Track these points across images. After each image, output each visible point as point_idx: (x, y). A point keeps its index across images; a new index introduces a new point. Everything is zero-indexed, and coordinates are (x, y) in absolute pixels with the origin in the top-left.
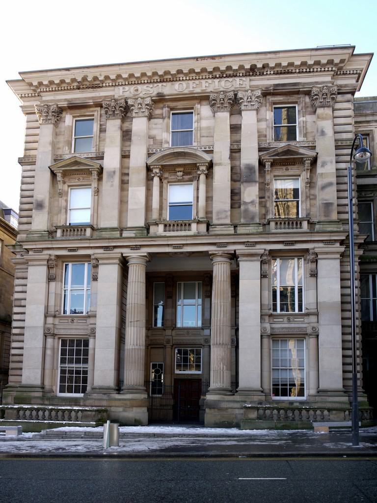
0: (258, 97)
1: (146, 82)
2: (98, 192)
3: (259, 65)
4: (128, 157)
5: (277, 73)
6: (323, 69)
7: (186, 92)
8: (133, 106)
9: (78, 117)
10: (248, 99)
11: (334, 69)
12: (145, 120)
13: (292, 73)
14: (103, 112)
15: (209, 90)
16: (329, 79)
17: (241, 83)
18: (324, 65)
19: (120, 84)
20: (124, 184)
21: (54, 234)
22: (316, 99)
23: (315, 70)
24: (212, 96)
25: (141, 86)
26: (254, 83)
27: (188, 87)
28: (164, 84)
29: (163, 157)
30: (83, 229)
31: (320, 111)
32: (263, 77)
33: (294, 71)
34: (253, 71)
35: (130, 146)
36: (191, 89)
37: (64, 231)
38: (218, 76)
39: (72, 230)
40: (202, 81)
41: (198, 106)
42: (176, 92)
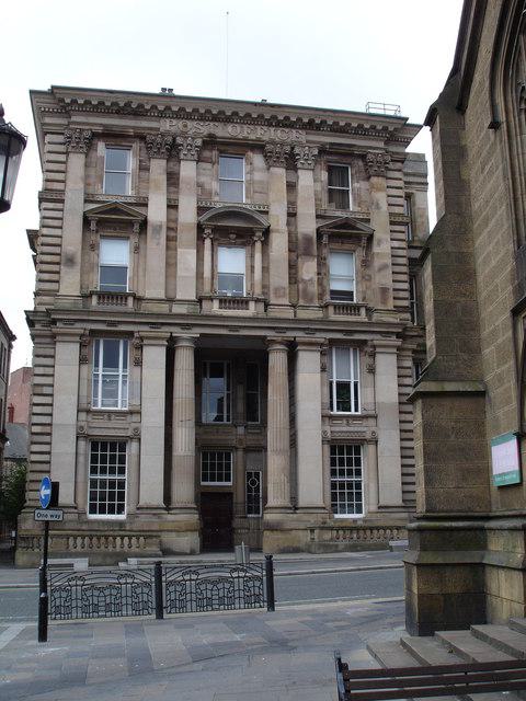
3: (318, 121)
13: (347, 132)
16: (382, 145)
18: (379, 131)
20: (171, 240)
24: (269, 147)
26: (311, 138)
31: (374, 180)
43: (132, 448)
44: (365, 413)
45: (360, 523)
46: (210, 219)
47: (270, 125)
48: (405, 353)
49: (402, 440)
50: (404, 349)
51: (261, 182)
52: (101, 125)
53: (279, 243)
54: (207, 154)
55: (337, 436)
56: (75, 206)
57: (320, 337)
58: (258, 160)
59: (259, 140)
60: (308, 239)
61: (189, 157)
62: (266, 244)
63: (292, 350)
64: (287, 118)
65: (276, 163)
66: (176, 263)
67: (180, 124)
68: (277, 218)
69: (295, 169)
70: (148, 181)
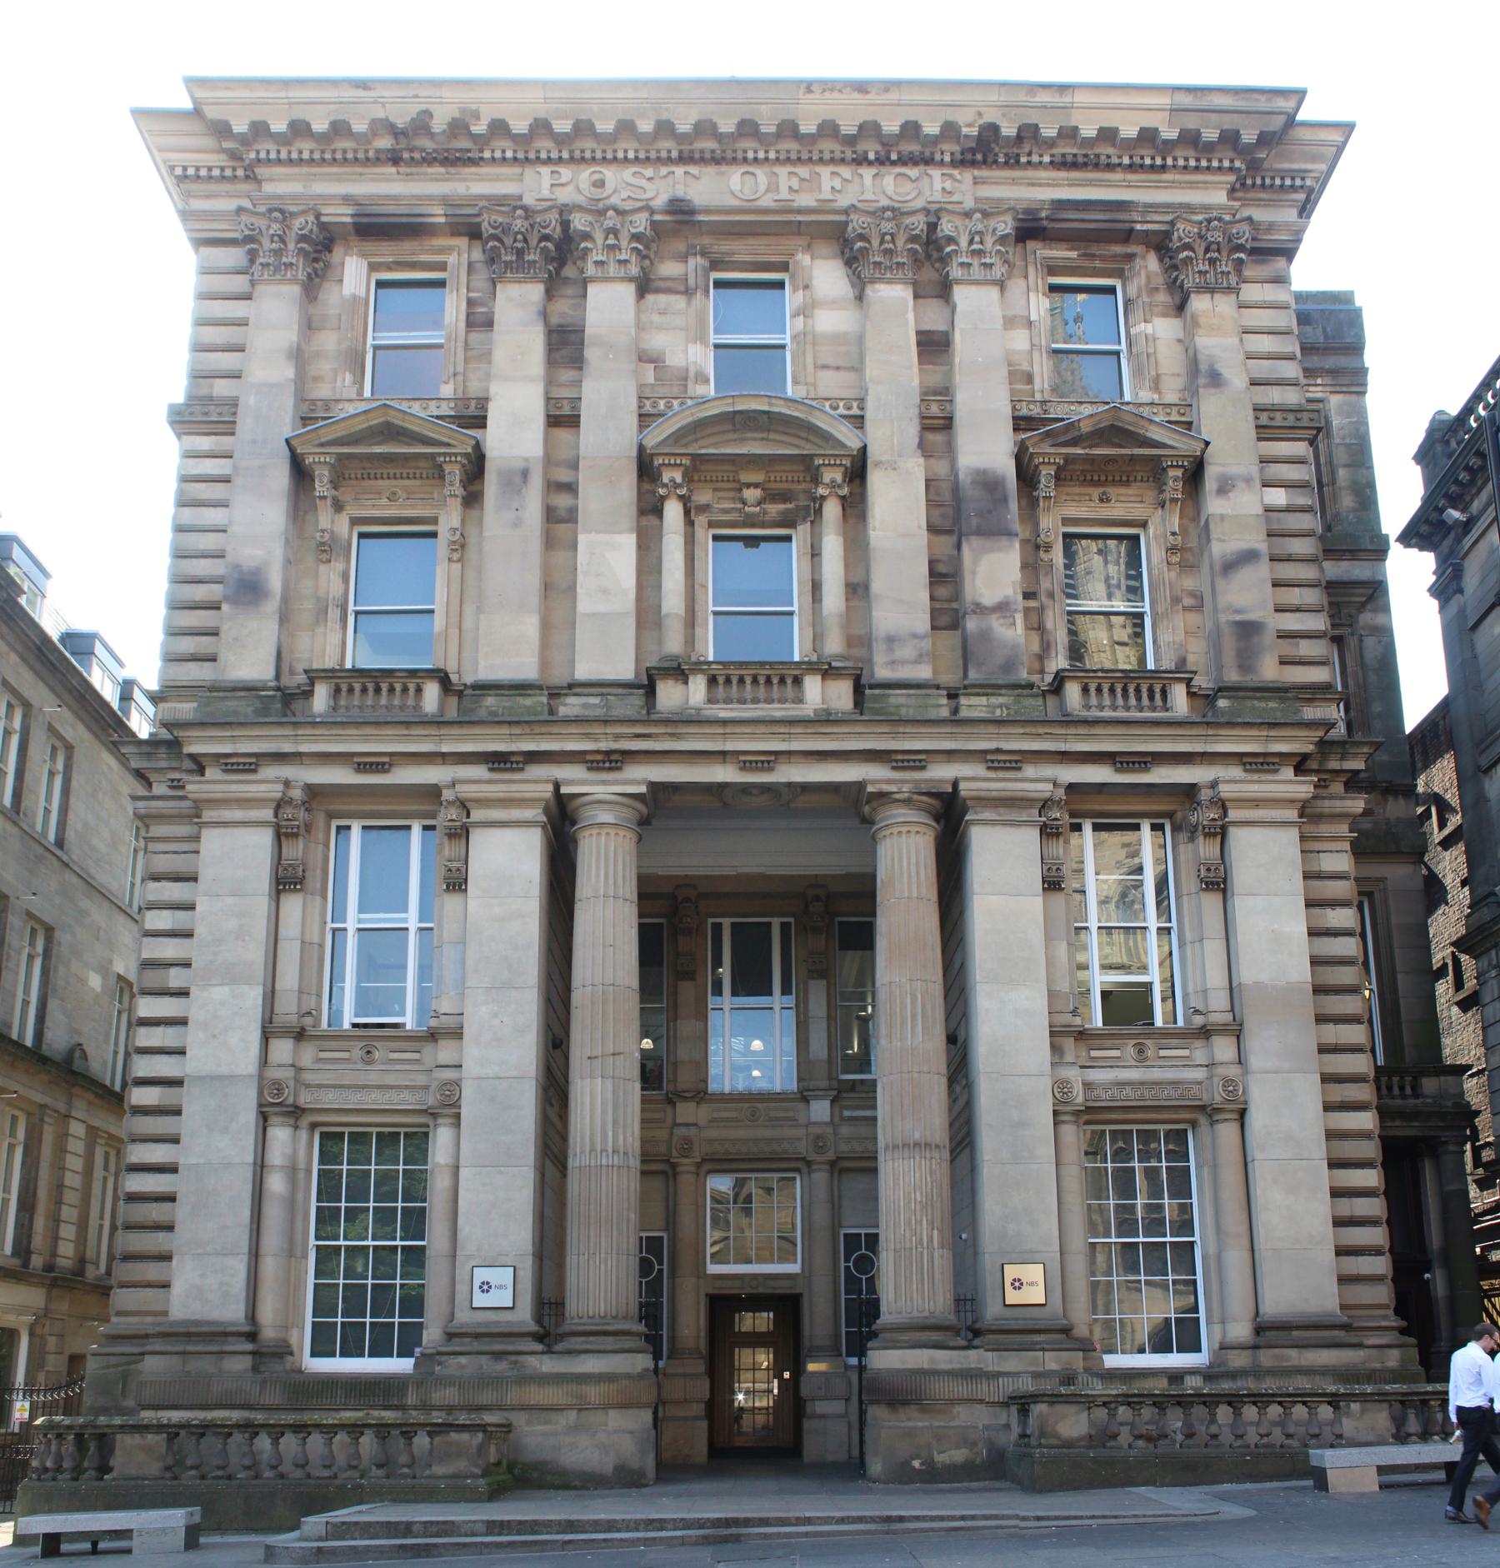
0: (1002, 240)
1: (631, 155)
2: (463, 546)
6: (1204, 163)
7: (767, 202)
8: (587, 236)
9: (389, 267)
10: (971, 242)
11: (1237, 164)
12: (628, 291)
13: (1110, 167)
14: (477, 255)
15: (843, 202)
16: (1220, 197)
17: (948, 185)
18: (1209, 148)
19: (543, 155)
21: (297, 705)
23: (1181, 162)
25: (613, 168)
27: (773, 187)
29: (698, 428)
30: (412, 688)
32: (1017, 174)
33: (1115, 160)
34: (984, 150)
35: (578, 383)
36: (784, 194)
37: (338, 690)
38: (871, 156)
39: (371, 687)
40: (818, 169)
41: (804, 259)
42: (735, 203)
43: (442, 1140)
44: (1198, 1020)
45: (1193, 1383)
46: (678, 436)
47: (861, 161)
48: (1325, 829)
49: (1328, 1107)
50: (1317, 818)
52: (347, 199)
53: (898, 503)
54: (669, 269)
55: (1104, 1098)
56: (269, 421)
57: (1039, 780)
58: (826, 275)
59: (823, 207)
60: (989, 484)
61: (612, 269)
62: (855, 505)
65: (886, 271)
66: (572, 588)
67: (586, 175)
68: (891, 435)
69: (943, 290)
70: (486, 357)
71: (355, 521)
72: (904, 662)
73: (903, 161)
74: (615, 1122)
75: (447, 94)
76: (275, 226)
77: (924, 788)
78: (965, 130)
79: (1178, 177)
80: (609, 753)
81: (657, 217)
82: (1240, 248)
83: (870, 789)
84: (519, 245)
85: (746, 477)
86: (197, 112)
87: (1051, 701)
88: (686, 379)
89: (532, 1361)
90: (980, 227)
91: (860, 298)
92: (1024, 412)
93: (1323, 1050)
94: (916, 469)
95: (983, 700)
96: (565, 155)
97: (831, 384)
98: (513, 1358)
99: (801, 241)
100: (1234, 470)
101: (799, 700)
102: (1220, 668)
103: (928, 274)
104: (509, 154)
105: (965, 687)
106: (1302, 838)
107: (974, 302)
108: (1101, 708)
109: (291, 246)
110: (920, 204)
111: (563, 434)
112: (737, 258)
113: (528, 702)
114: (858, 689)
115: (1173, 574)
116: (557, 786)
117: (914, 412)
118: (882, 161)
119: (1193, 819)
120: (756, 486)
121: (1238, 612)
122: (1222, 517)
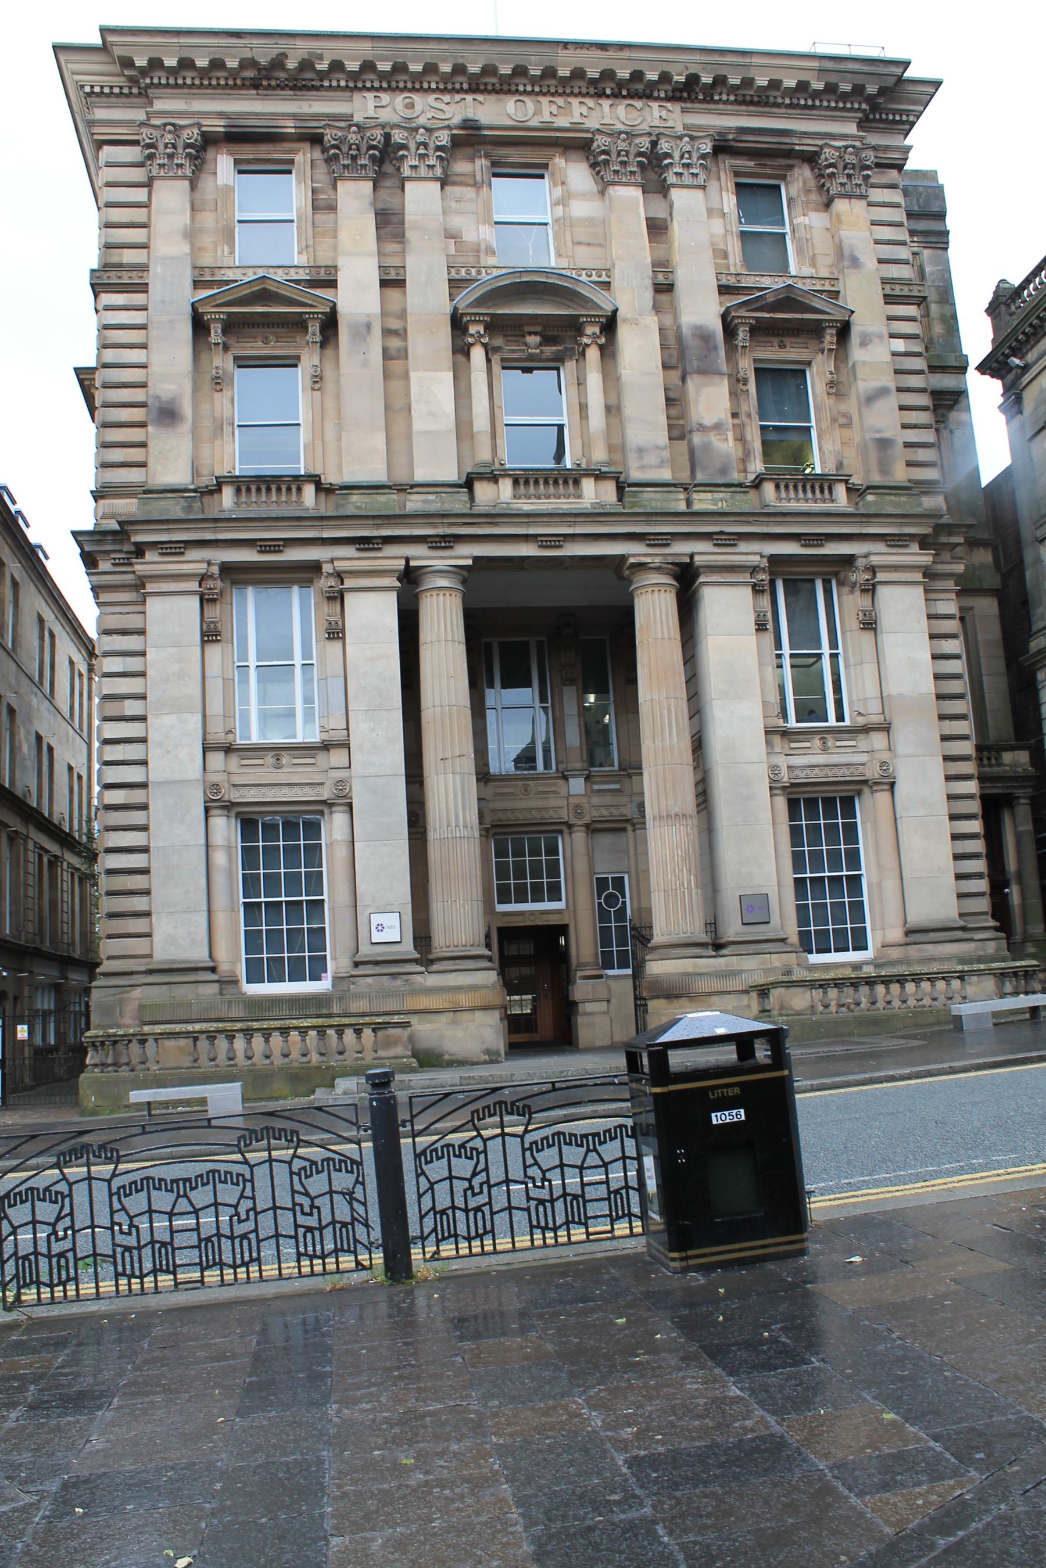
0: (703, 157)
3: (707, 79)
4: (400, 283)
5: (743, 103)
7: (534, 123)
8: (404, 147)
10: (682, 157)
13: (776, 105)
16: (852, 129)
17: (664, 114)
22: (832, 175)
24: (601, 142)
25: (420, 94)
28: (480, 97)
32: (712, 106)
33: (780, 100)
34: (688, 91)
36: (547, 118)
40: (570, 99)
42: (512, 123)
43: (334, 828)
44: (861, 721)
45: (869, 970)
46: (480, 301)
47: (600, 95)
48: (940, 585)
49: (948, 778)
51: (590, 221)
52: (221, 115)
53: (639, 347)
54: (461, 167)
55: (802, 777)
58: (577, 173)
59: (575, 127)
60: (704, 336)
61: (423, 172)
62: (608, 351)
63: (686, 581)
64: (637, 76)
67: (400, 99)
68: (630, 297)
69: (664, 189)
71: (236, 358)
72: (650, 467)
73: (631, 96)
74: (464, 806)
75: (300, 43)
76: (170, 136)
77: (670, 559)
78: (676, 78)
79: (823, 113)
80: (443, 537)
81: (455, 132)
82: (868, 168)
83: (632, 560)
84: (354, 153)
85: (527, 329)
86: (104, 48)
87: (753, 494)
88: (478, 251)
89: (419, 979)
90: (688, 148)
91: (602, 193)
92: (724, 282)
93: (944, 738)
94: (652, 322)
95: (709, 496)
96: (385, 85)
97: (585, 257)
98: (405, 977)
99: (561, 150)
100: (871, 329)
101: (580, 497)
102: (867, 471)
103: (652, 176)
104: (343, 83)
105: (696, 486)
106: (926, 591)
107: (685, 201)
108: (789, 500)
109: (180, 150)
110: (645, 127)
111: (393, 293)
112: (510, 160)
113: (383, 499)
114: (620, 489)
115: (831, 401)
116: (407, 560)
117: (649, 283)
118: (616, 95)
119: (853, 579)
120: (535, 334)
121: (878, 431)
122: (864, 363)
